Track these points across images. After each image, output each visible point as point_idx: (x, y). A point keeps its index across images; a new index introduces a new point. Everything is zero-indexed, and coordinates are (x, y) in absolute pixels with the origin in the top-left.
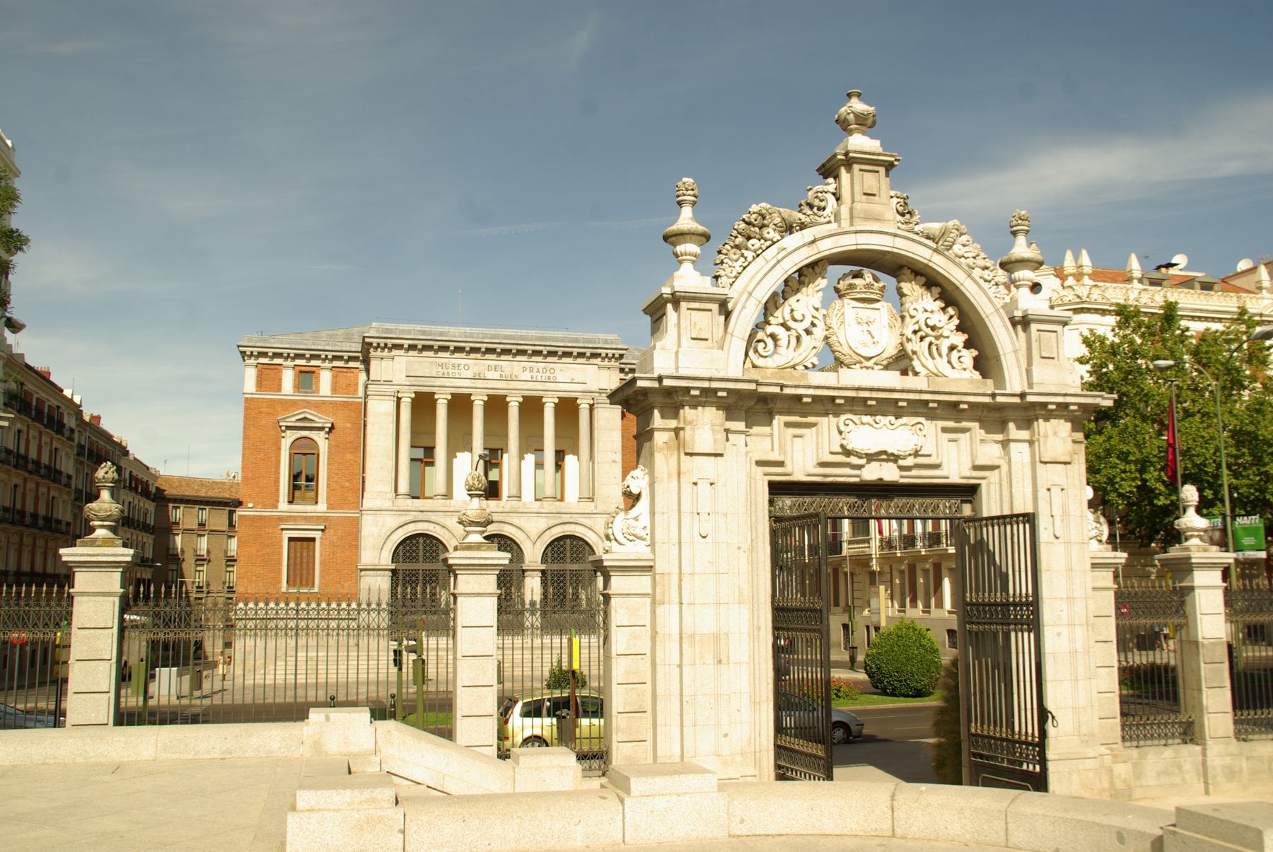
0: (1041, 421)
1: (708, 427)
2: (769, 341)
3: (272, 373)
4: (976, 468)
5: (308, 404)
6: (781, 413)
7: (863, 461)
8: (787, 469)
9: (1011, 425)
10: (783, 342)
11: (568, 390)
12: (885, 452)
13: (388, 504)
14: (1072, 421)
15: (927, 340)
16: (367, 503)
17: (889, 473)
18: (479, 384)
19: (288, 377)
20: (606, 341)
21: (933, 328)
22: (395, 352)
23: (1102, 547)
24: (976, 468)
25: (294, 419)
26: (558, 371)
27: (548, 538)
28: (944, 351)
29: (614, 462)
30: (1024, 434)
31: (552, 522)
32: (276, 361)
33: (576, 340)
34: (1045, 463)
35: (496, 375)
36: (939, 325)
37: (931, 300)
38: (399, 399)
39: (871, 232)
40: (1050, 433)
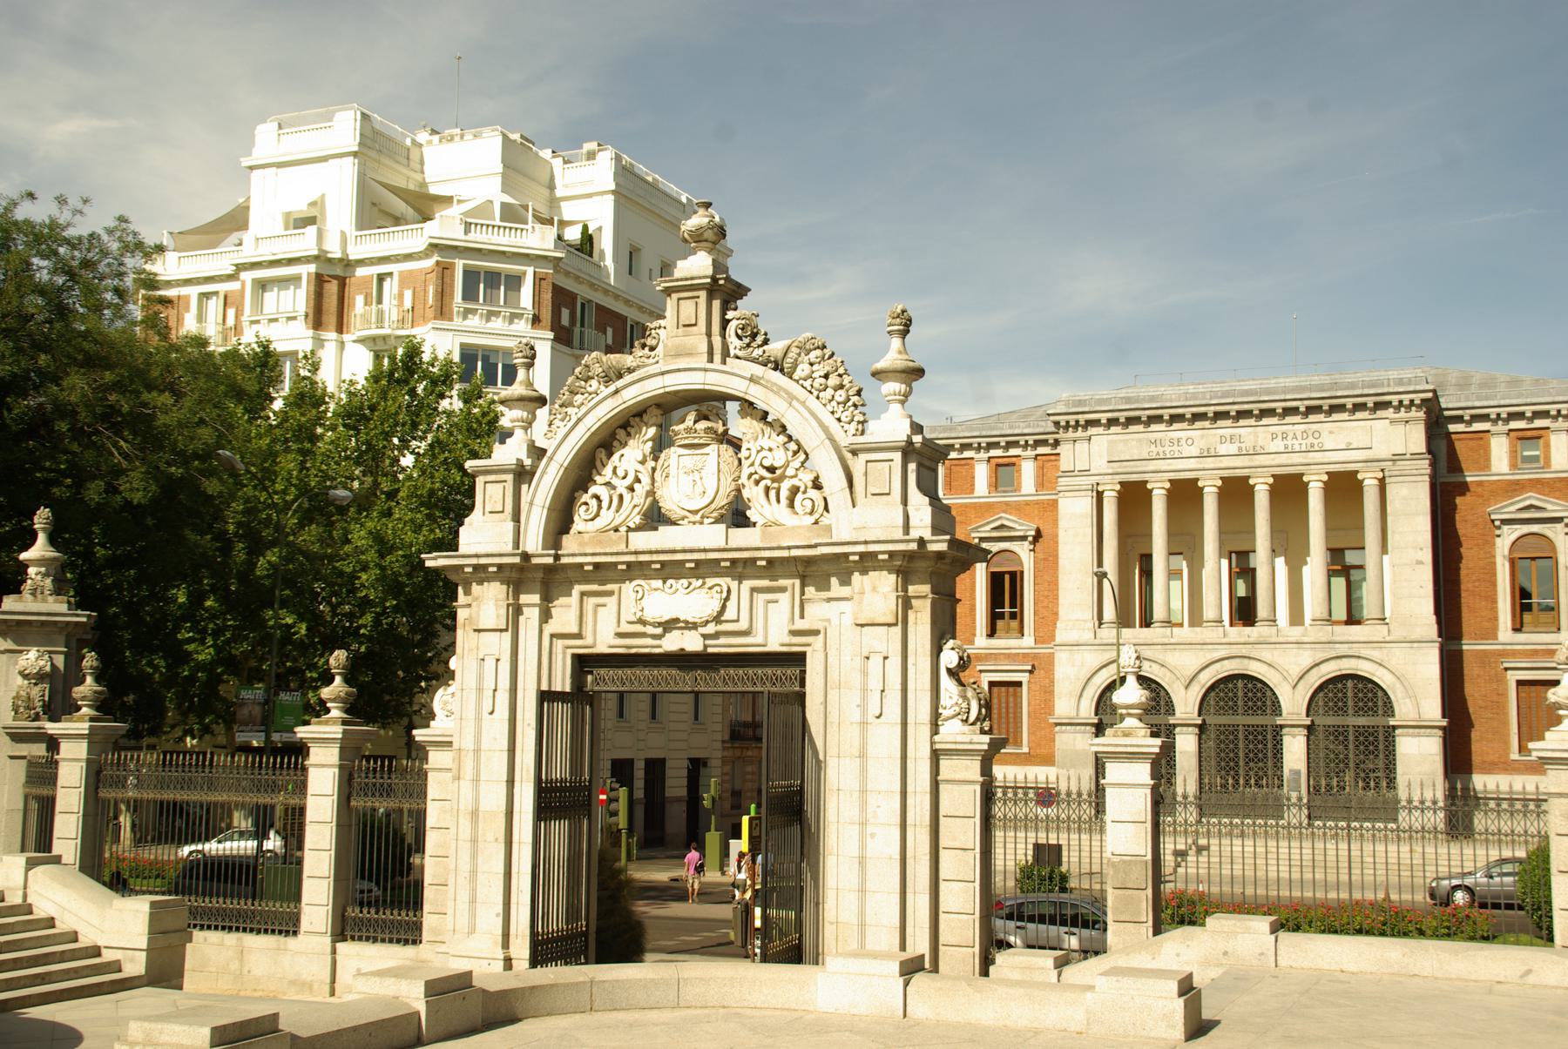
0: (856, 574)
1: (492, 603)
2: (594, 503)
3: (963, 470)
4: (794, 633)
5: (1007, 507)
6: (580, 583)
7: (659, 631)
8: (589, 641)
9: (834, 581)
10: (605, 504)
11: (1341, 460)
12: (677, 620)
13: (1087, 636)
14: (898, 572)
15: (763, 483)
16: (1060, 637)
17: (691, 642)
18: (1209, 463)
19: (1028, 470)
20: (1400, 382)
21: (772, 470)
22: (1092, 431)
23: (967, 728)
24: (794, 633)
25: (988, 528)
26: (1325, 434)
27: (1315, 679)
28: (784, 494)
29: (1420, 562)
30: (845, 591)
31: (1321, 656)
32: (967, 454)
33: (1352, 386)
34: (862, 625)
35: (1233, 449)
36: (776, 465)
37: (774, 435)
38: (1100, 495)
39: (679, 370)
40: (868, 588)
